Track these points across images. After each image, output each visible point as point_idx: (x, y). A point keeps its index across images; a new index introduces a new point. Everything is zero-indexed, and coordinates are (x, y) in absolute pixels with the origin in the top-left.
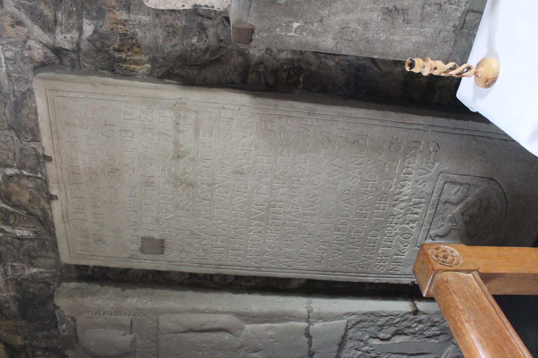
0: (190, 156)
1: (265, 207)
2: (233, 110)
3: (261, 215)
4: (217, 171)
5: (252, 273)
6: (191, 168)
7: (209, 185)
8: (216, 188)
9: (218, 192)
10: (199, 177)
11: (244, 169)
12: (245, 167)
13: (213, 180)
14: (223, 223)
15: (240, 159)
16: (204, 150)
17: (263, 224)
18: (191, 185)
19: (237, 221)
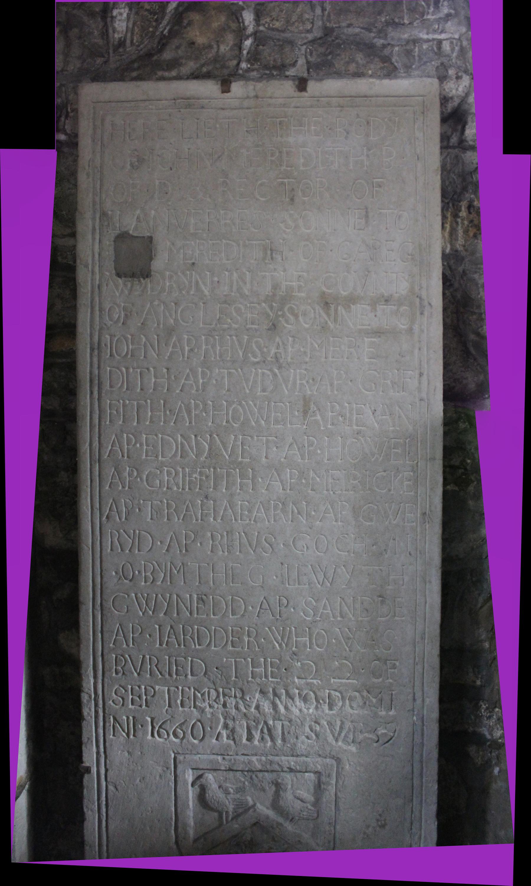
0: (329, 322)
1: (240, 459)
2: (419, 389)
3: (222, 455)
4: (306, 370)
5: (84, 449)
6: (307, 326)
7: (276, 358)
8: (271, 370)
9: (263, 374)
10: (290, 339)
11: (315, 415)
12: (319, 417)
13: (288, 364)
14: (198, 387)
15: (333, 407)
16: (343, 347)
17: (202, 459)
18: (274, 327)
19: (205, 410)
